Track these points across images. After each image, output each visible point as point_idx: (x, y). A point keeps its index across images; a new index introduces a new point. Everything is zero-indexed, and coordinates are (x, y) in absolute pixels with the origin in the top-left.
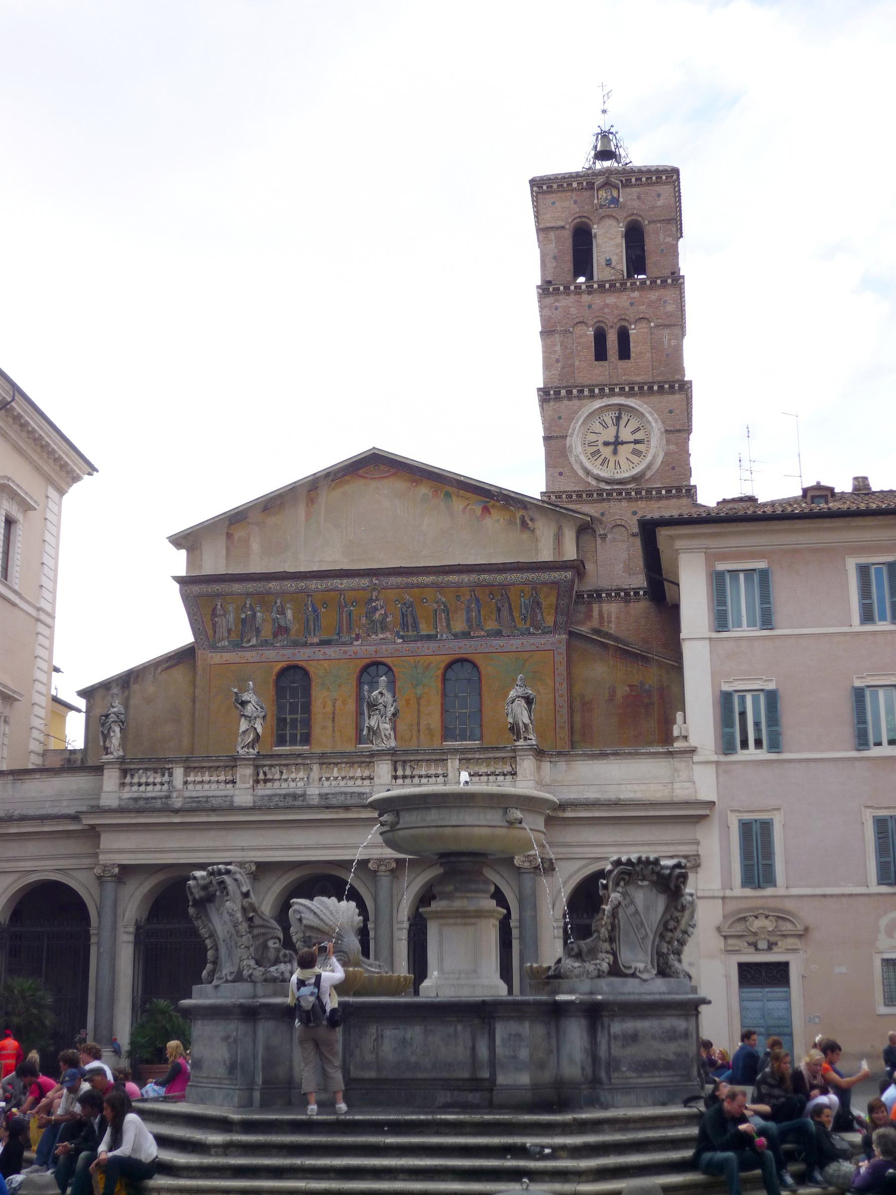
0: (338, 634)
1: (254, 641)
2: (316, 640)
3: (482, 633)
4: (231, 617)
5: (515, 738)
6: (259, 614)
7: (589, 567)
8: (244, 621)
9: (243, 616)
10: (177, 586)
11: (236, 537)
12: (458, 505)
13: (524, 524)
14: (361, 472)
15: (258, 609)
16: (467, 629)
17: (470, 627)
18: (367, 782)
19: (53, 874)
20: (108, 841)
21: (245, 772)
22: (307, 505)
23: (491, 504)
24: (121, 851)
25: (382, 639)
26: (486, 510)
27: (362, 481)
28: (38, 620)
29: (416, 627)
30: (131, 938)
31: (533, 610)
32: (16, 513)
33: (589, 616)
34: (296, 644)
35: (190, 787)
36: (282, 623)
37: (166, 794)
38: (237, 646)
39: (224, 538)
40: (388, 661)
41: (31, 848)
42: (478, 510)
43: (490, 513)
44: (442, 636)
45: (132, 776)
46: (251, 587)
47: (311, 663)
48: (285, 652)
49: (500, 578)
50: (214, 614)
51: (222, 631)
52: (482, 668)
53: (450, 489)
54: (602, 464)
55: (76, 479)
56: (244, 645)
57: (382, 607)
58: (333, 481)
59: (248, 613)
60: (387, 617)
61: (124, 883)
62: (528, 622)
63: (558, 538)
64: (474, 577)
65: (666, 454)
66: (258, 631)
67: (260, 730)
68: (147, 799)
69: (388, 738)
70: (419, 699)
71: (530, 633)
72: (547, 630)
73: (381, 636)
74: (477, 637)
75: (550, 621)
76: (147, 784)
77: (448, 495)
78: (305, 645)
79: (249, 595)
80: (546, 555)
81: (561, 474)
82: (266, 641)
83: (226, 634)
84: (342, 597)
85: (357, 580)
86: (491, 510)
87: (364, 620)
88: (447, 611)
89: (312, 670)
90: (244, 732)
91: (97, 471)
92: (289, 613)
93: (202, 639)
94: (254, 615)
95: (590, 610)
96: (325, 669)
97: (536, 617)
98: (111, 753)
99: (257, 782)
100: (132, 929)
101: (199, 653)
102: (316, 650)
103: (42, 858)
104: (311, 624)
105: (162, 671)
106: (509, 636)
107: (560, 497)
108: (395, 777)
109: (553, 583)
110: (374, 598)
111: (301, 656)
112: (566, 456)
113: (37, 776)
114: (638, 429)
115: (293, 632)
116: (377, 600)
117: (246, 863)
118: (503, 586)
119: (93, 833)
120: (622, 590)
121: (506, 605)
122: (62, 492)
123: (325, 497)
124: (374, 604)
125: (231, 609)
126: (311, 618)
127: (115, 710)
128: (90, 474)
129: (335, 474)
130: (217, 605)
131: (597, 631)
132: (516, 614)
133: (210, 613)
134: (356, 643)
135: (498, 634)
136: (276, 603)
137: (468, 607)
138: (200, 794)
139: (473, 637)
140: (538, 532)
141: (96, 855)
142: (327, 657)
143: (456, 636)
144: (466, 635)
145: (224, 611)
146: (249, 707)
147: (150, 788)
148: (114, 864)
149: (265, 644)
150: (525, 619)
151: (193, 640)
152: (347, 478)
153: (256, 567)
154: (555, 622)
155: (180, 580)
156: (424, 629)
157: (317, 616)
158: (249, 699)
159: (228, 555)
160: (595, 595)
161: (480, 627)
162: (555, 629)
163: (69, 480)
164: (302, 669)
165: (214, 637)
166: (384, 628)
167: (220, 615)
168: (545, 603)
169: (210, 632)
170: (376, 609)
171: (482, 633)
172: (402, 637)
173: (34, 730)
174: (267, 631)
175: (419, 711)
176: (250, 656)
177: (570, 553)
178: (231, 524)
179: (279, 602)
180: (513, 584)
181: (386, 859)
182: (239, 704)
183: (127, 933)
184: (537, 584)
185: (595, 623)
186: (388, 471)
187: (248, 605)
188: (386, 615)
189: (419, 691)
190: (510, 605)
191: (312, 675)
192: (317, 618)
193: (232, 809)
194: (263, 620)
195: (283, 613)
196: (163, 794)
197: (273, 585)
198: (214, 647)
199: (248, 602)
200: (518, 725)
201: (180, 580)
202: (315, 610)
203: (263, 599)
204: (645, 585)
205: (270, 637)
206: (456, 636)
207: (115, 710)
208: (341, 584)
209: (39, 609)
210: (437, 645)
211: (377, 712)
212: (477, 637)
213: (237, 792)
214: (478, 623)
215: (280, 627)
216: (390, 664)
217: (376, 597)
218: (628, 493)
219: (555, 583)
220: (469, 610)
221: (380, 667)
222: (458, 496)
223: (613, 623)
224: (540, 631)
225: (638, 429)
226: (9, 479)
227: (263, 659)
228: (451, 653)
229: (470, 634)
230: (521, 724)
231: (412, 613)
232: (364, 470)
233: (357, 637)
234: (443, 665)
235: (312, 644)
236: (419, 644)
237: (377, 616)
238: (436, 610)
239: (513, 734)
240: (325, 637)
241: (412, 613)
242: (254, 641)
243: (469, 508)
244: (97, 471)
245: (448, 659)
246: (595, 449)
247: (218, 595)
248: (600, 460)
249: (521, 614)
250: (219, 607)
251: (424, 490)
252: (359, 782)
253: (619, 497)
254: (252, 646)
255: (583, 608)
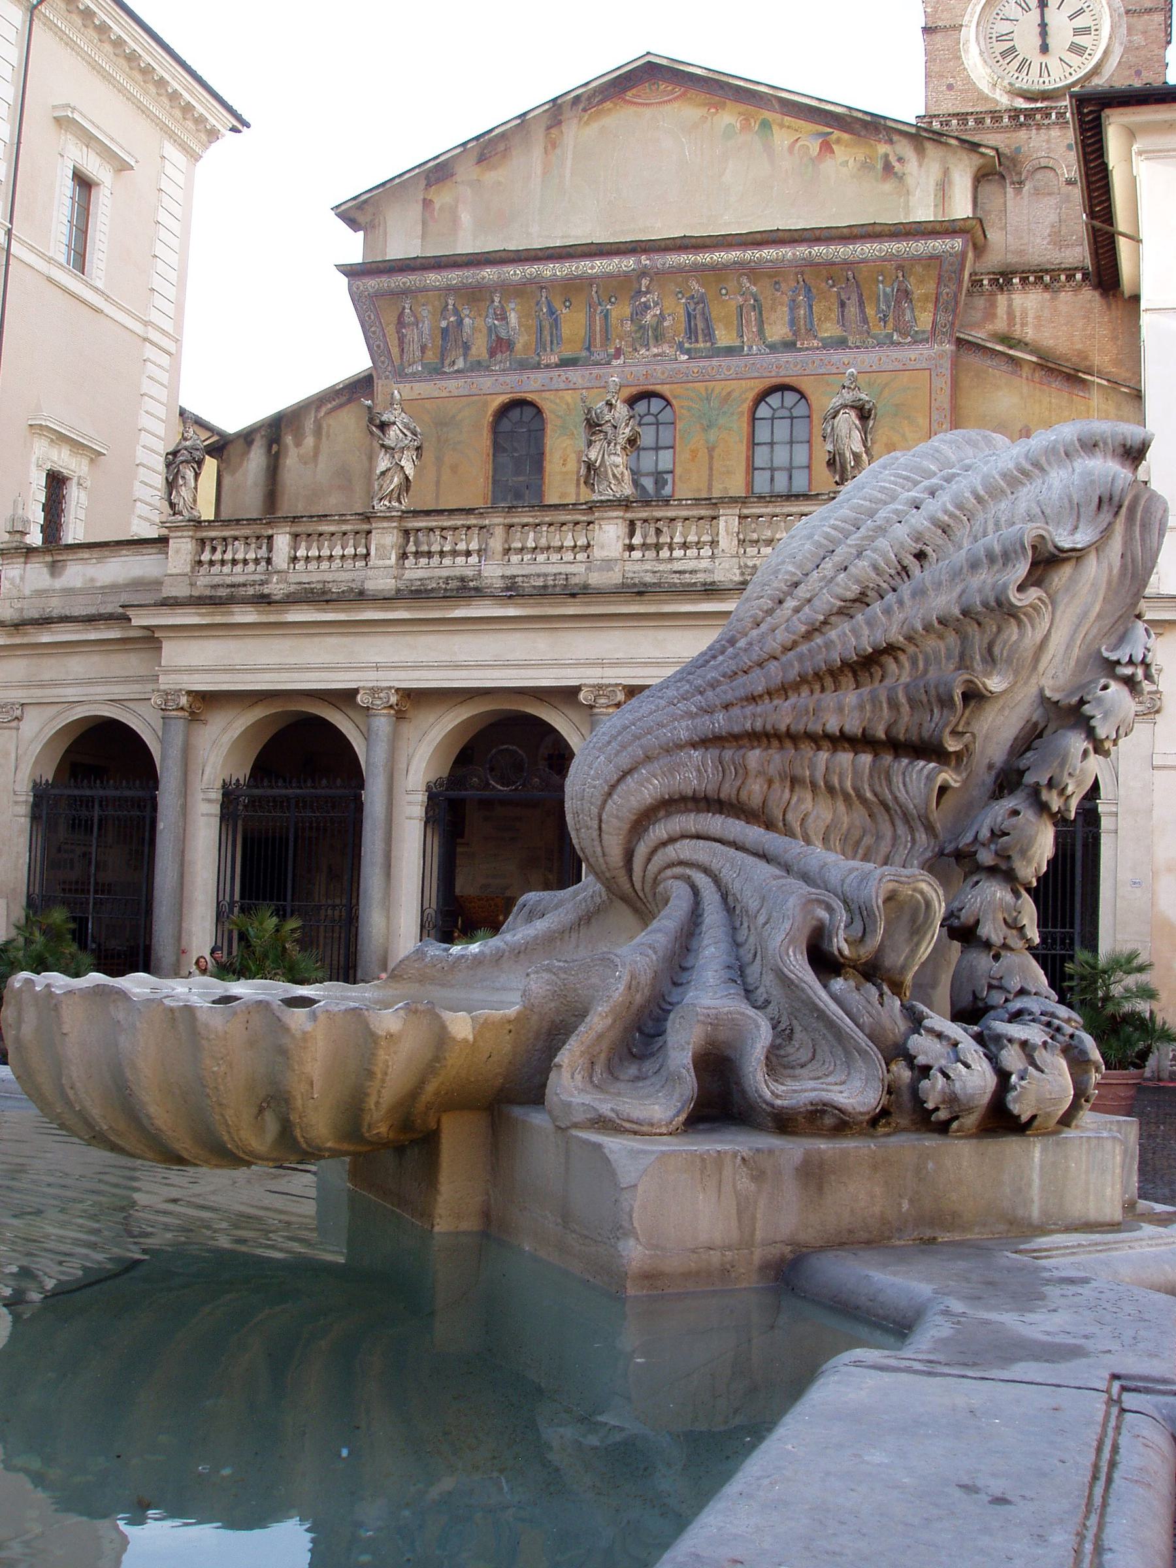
0: (588, 349)
1: (460, 364)
2: (554, 359)
3: (815, 343)
4: (426, 326)
5: (837, 478)
6: (467, 321)
7: (994, 236)
8: (445, 332)
9: (444, 324)
10: (345, 280)
11: (437, 206)
12: (781, 139)
13: (888, 168)
14: (629, 95)
15: (467, 312)
16: (790, 337)
17: (796, 333)
18: (581, 556)
19: (107, 707)
20: (174, 652)
21: (385, 539)
22: (546, 152)
23: (834, 137)
24: (191, 670)
25: (655, 355)
26: (826, 147)
27: (632, 109)
28: (146, 339)
29: (709, 335)
30: (216, 809)
31: (898, 302)
32: (94, 167)
33: (990, 315)
34: (524, 366)
35: (300, 566)
36: (503, 335)
37: (263, 577)
38: (436, 371)
39: (419, 207)
40: (665, 390)
41: (77, 666)
42: (814, 146)
43: (832, 152)
44: (750, 348)
45: (214, 550)
46: (454, 277)
47: (546, 395)
48: (508, 379)
49: (841, 251)
50: (400, 323)
51: (414, 349)
52: (812, 399)
53: (766, 114)
54: (1019, 70)
55: (213, 135)
56: (446, 369)
57: (656, 304)
58: (585, 110)
59: (452, 319)
60: (664, 319)
61: (205, 722)
62: (890, 324)
63: (943, 188)
64: (802, 251)
65: (1127, 50)
66: (466, 347)
67: (409, 470)
68: (233, 586)
69: (619, 481)
70: (711, 450)
71: (892, 343)
72: (921, 337)
73: (655, 351)
74: (807, 349)
75: (925, 320)
76: (234, 562)
77: (765, 125)
78: (537, 366)
79: (449, 289)
80: (923, 212)
81: (950, 87)
82: (479, 362)
83: (418, 353)
84: (594, 289)
85: (616, 261)
86: (834, 147)
87: (628, 326)
88: (758, 307)
89: (546, 406)
90: (383, 473)
91: (248, 125)
92: (513, 318)
93: (383, 362)
94: (460, 322)
95: (993, 305)
96: (568, 404)
97: (904, 315)
98: (180, 513)
99: (404, 556)
100: (216, 795)
101: (379, 385)
102: (555, 373)
103: (91, 682)
104: (546, 333)
105: (328, 413)
106: (858, 347)
107: (948, 123)
108: (631, 548)
109: (931, 257)
110: (643, 289)
111: (530, 385)
112: (960, 58)
113: (86, 556)
114: (1081, 11)
115: (519, 346)
116: (647, 292)
117: (382, 689)
118: (848, 264)
119: (151, 640)
120: (1047, 271)
121: (855, 297)
122: (195, 157)
123: (574, 133)
124: (643, 300)
125: (425, 313)
126: (546, 324)
127: (188, 443)
128: (234, 130)
129: (589, 98)
130: (404, 308)
131: (1005, 339)
132: (870, 311)
133: (395, 319)
134: (615, 363)
135: (841, 343)
136: (493, 301)
137: (794, 301)
138: (315, 577)
139: (800, 350)
140: (910, 181)
141: (155, 678)
142: (571, 386)
143: (773, 348)
144: (789, 346)
145: (416, 317)
146: (393, 432)
147: (239, 568)
148: (181, 690)
149: (477, 366)
150: (884, 320)
151: (368, 364)
152: (608, 105)
153: (466, 245)
154: (934, 323)
155: (351, 272)
156: (724, 337)
157: (556, 320)
158: (392, 419)
159: (424, 236)
160: (1001, 281)
161: (811, 332)
162: (934, 333)
163: (204, 137)
164: (531, 404)
165: (402, 358)
166: (659, 338)
167: (409, 324)
168: (918, 292)
169: (395, 351)
170: (647, 307)
171: (815, 343)
172: (687, 352)
173: (138, 504)
174: (480, 348)
175: (711, 469)
176: (453, 385)
177: (961, 208)
178: (429, 185)
179: (497, 299)
180: (863, 261)
181: (610, 685)
182: (376, 426)
183: (209, 801)
184: (904, 259)
185: (1000, 324)
186: (672, 92)
187: (450, 307)
188: (662, 317)
189: (713, 435)
190: (861, 296)
191: (547, 414)
192: (556, 323)
193: (360, 597)
194: (474, 329)
195: (504, 318)
196: (257, 577)
197: (489, 274)
198: (401, 375)
199: (451, 302)
200: (842, 455)
201: (351, 272)
202: (552, 312)
203: (475, 295)
204: (1088, 263)
205: (485, 355)
206: (773, 348)
207: (188, 443)
208: (592, 268)
209: (146, 323)
210: (742, 364)
211: (602, 436)
212: (807, 349)
213: (370, 573)
214: (808, 327)
215: (499, 340)
216: (668, 394)
217: (648, 287)
218: (1061, 115)
219: (934, 259)
220: (793, 306)
221: (654, 401)
222: (782, 126)
223: (1030, 326)
224: (909, 340)
225: (1081, 11)
226: (74, 109)
227: (475, 391)
228: (765, 375)
229: (794, 344)
230: (848, 454)
231: (703, 314)
232: (634, 91)
233: (617, 354)
234: (751, 395)
235: (547, 366)
236: (715, 362)
237: (648, 318)
238: (741, 307)
239: (835, 472)
240: (567, 354)
241: (703, 314)
242: (460, 364)
243: (799, 144)
244: (248, 125)
245: (760, 386)
246: (1008, 45)
247: (405, 292)
248: (1016, 64)
249: (879, 311)
250: (407, 311)
251: (728, 117)
252: (569, 556)
253: (1046, 122)
254: (457, 371)
255: (980, 302)
